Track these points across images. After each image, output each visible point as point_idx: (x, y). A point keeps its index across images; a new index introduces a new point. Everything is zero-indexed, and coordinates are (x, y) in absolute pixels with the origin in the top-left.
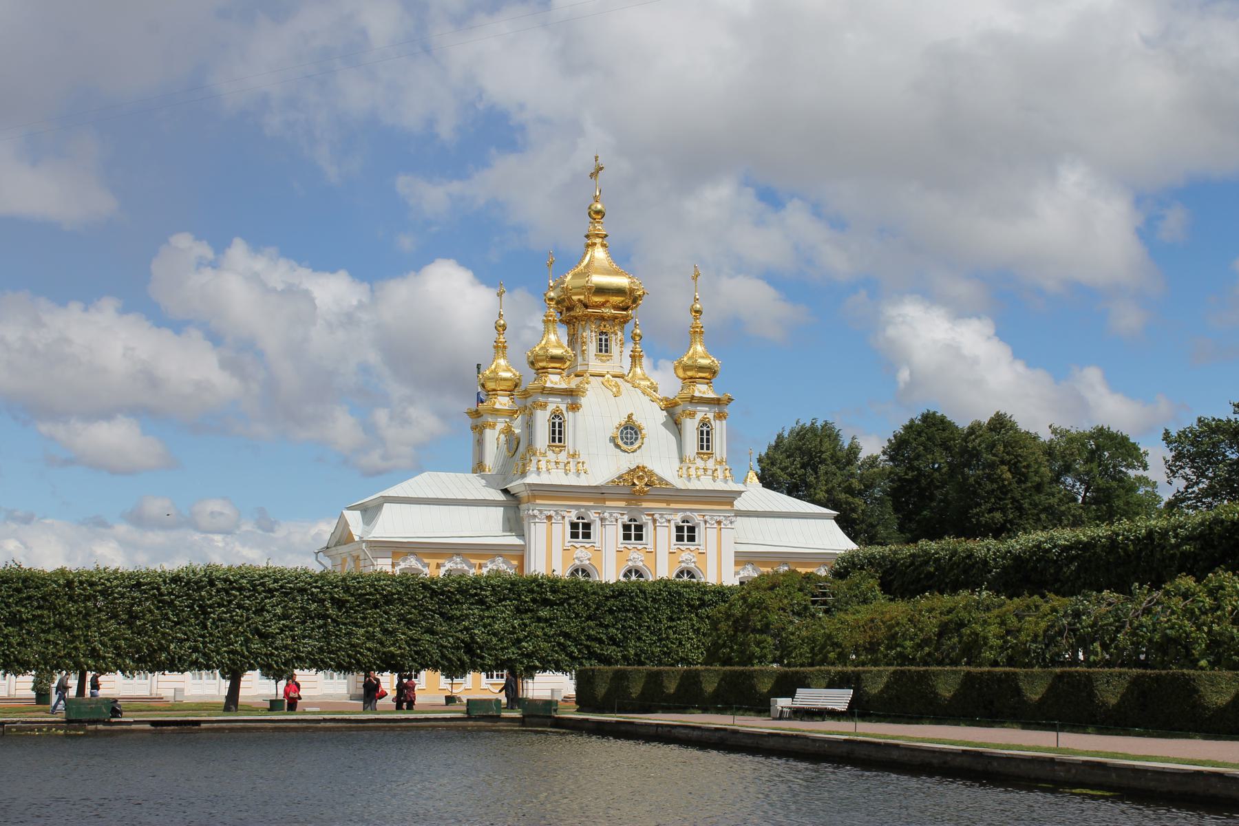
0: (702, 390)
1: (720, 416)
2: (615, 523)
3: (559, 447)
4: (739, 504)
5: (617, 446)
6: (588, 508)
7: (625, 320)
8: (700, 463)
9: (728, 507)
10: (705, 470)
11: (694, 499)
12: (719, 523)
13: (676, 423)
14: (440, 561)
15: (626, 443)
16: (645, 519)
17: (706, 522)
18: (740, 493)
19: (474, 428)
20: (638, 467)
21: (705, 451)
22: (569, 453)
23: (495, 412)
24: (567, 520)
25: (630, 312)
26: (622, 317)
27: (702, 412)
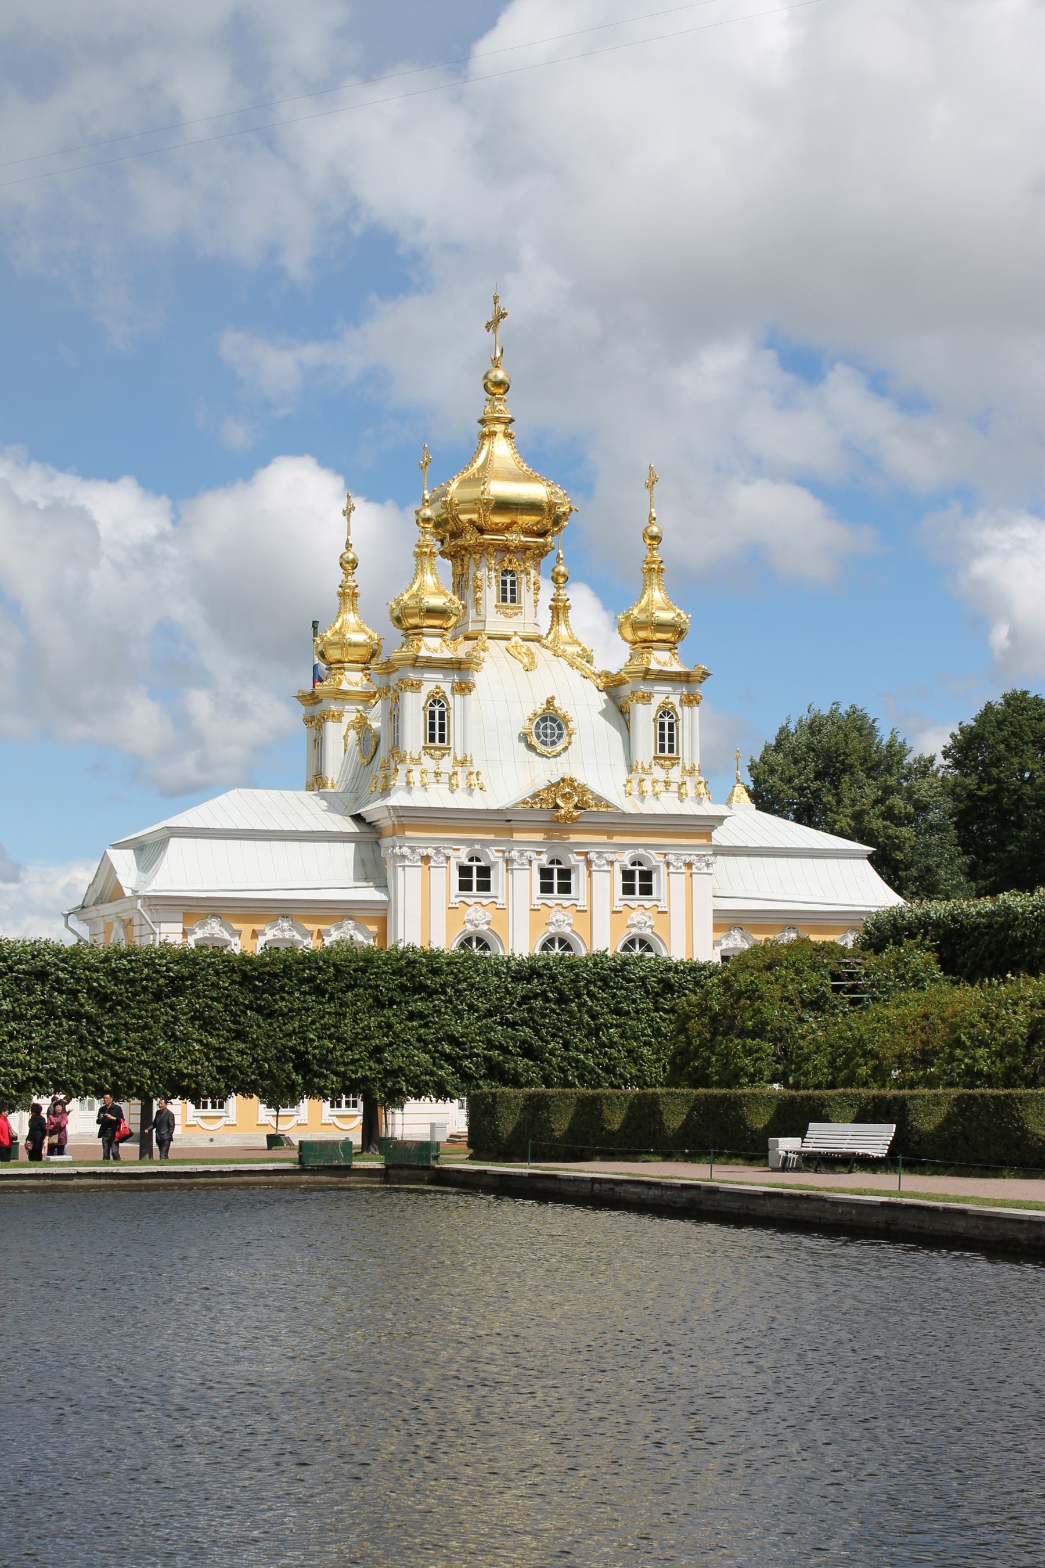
0: (661, 660)
1: (690, 700)
2: (527, 867)
3: (440, 749)
4: (720, 836)
5: (531, 747)
6: (485, 843)
7: (541, 552)
8: (659, 773)
9: (704, 842)
10: (667, 783)
11: (649, 829)
12: (689, 865)
13: (621, 711)
14: (258, 927)
15: (544, 743)
16: (574, 860)
17: (668, 864)
18: (721, 819)
19: (309, 720)
20: (563, 780)
21: (666, 754)
22: (455, 758)
23: (341, 696)
24: (453, 863)
25: (550, 539)
26: (538, 548)
27: (663, 694)
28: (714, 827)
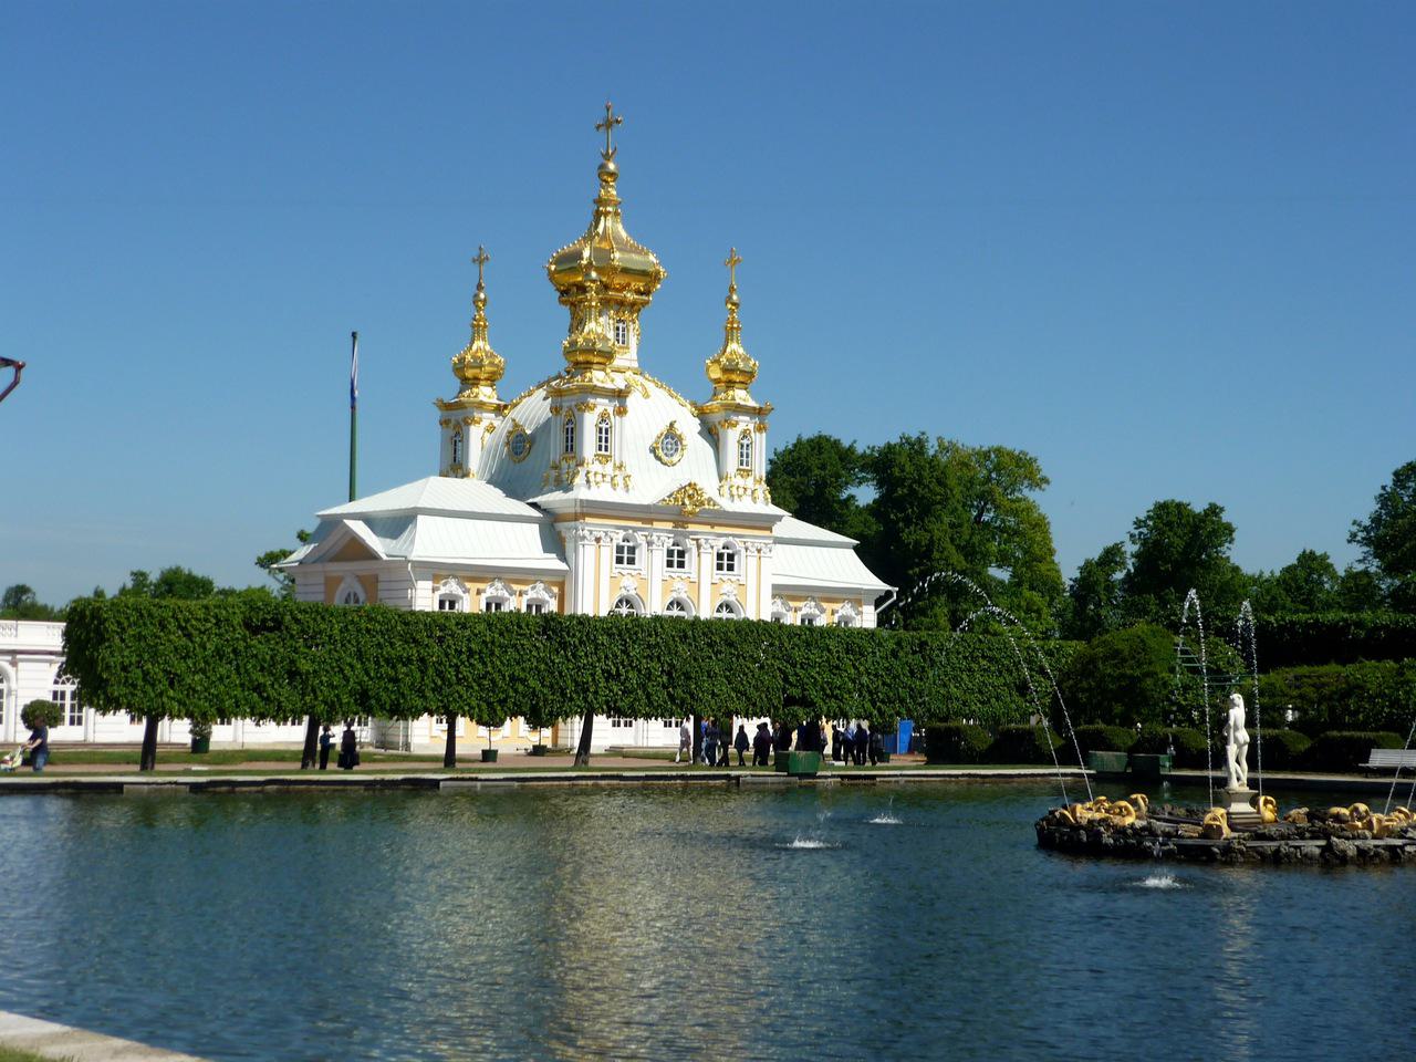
1: (760, 429)
4: (780, 530)
5: (658, 458)
6: (635, 530)
9: (767, 533)
12: (759, 551)
14: (481, 586)
15: (666, 455)
16: (690, 544)
17: (747, 549)
19: (445, 423)
20: (690, 485)
21: (603, 452)
23: (481, 406)
27: (745, 422)
28: (774, 523)
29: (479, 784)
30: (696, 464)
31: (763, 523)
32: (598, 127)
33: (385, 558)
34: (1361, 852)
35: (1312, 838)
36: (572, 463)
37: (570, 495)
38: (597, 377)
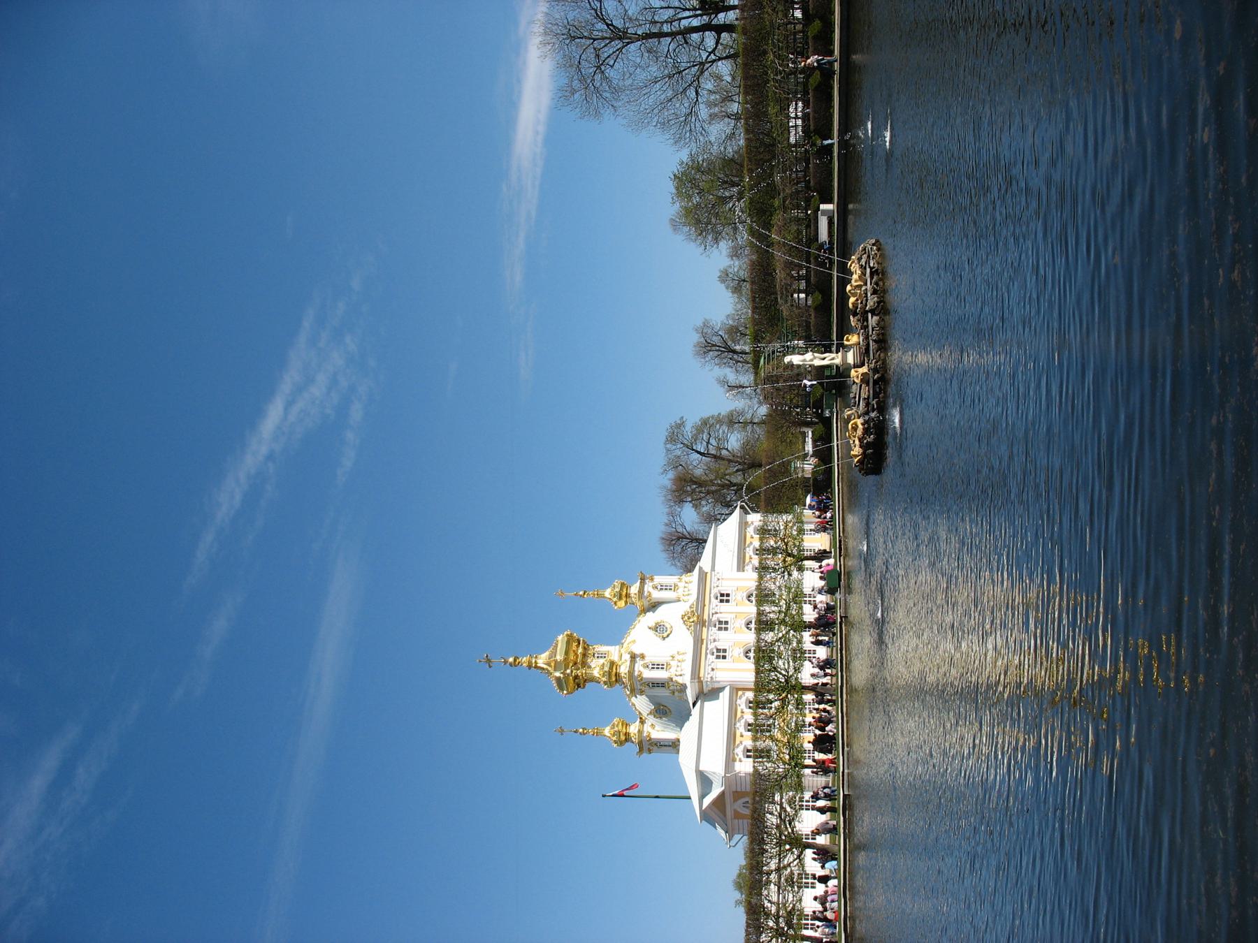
4: (707, 568)
5: (668, 636)
9: (708, 575)
15: (666, 631)
16: (715, 618)
17: (717, 586)
19: (650, 751)
20: (682, 618)
23: (640, 732)
27: (648, 587)
28: (703, 571)
29: (846, 771)
30: (670, 614)
31: (703, 577)
32: (490, 667)
33: (723, 788)
34: (875, 292)
35: (867, 322)
36: (671, 684)
37: (688, 685)
38: (624, 670)
